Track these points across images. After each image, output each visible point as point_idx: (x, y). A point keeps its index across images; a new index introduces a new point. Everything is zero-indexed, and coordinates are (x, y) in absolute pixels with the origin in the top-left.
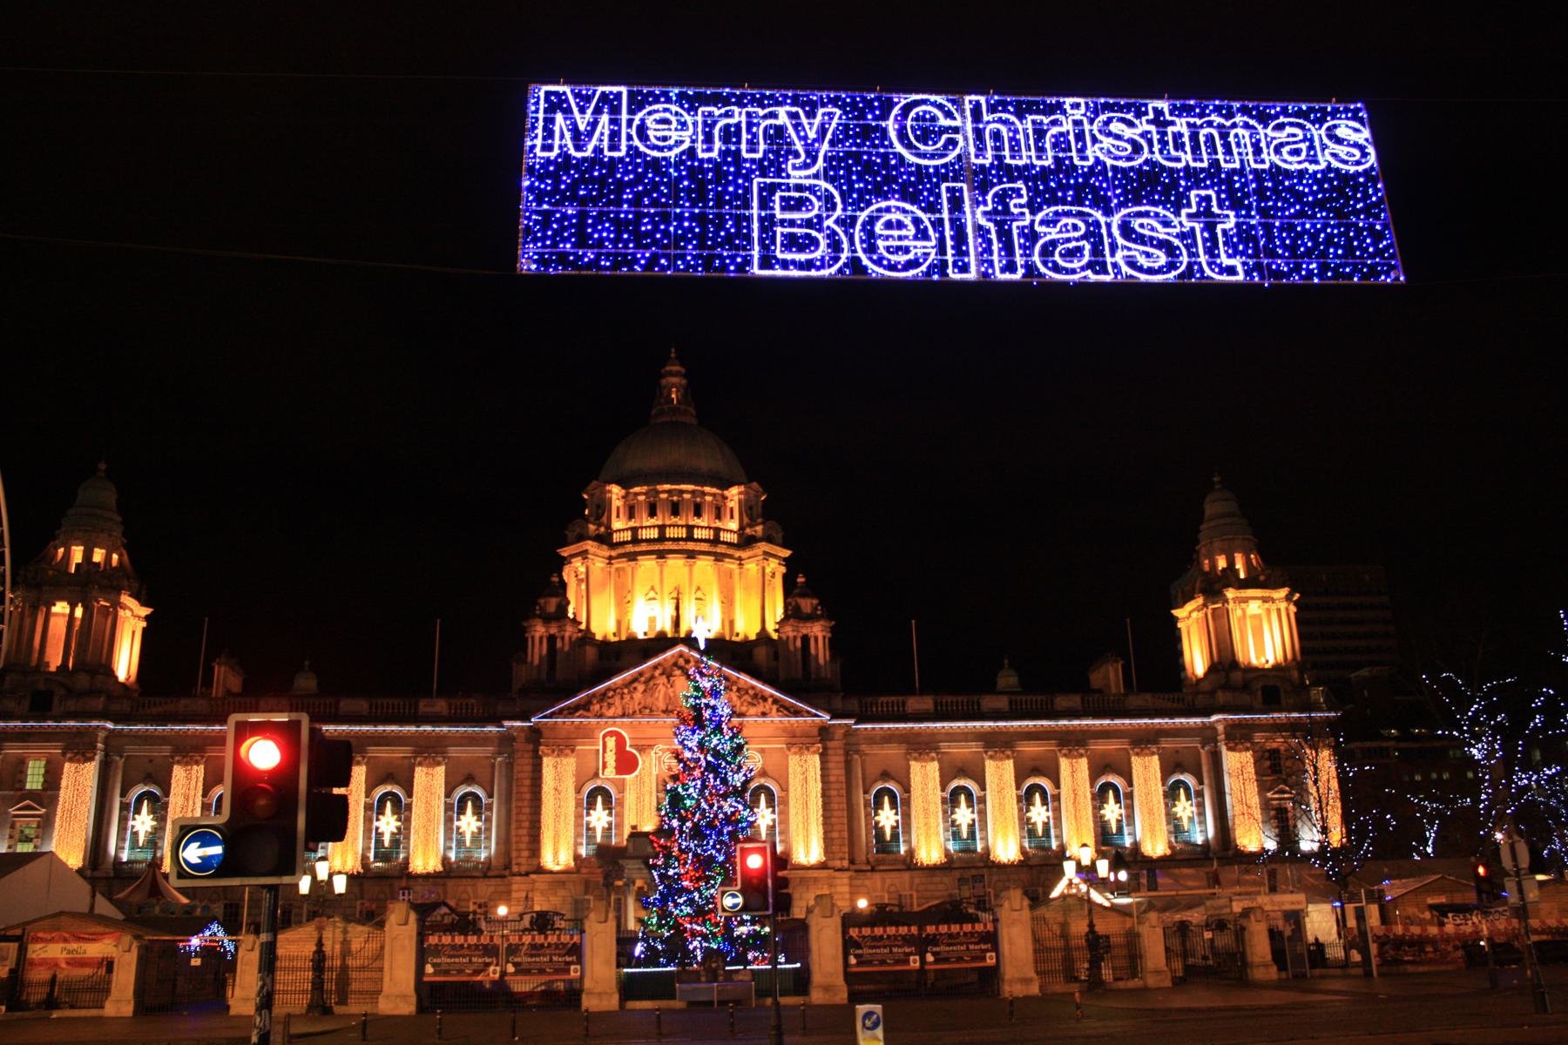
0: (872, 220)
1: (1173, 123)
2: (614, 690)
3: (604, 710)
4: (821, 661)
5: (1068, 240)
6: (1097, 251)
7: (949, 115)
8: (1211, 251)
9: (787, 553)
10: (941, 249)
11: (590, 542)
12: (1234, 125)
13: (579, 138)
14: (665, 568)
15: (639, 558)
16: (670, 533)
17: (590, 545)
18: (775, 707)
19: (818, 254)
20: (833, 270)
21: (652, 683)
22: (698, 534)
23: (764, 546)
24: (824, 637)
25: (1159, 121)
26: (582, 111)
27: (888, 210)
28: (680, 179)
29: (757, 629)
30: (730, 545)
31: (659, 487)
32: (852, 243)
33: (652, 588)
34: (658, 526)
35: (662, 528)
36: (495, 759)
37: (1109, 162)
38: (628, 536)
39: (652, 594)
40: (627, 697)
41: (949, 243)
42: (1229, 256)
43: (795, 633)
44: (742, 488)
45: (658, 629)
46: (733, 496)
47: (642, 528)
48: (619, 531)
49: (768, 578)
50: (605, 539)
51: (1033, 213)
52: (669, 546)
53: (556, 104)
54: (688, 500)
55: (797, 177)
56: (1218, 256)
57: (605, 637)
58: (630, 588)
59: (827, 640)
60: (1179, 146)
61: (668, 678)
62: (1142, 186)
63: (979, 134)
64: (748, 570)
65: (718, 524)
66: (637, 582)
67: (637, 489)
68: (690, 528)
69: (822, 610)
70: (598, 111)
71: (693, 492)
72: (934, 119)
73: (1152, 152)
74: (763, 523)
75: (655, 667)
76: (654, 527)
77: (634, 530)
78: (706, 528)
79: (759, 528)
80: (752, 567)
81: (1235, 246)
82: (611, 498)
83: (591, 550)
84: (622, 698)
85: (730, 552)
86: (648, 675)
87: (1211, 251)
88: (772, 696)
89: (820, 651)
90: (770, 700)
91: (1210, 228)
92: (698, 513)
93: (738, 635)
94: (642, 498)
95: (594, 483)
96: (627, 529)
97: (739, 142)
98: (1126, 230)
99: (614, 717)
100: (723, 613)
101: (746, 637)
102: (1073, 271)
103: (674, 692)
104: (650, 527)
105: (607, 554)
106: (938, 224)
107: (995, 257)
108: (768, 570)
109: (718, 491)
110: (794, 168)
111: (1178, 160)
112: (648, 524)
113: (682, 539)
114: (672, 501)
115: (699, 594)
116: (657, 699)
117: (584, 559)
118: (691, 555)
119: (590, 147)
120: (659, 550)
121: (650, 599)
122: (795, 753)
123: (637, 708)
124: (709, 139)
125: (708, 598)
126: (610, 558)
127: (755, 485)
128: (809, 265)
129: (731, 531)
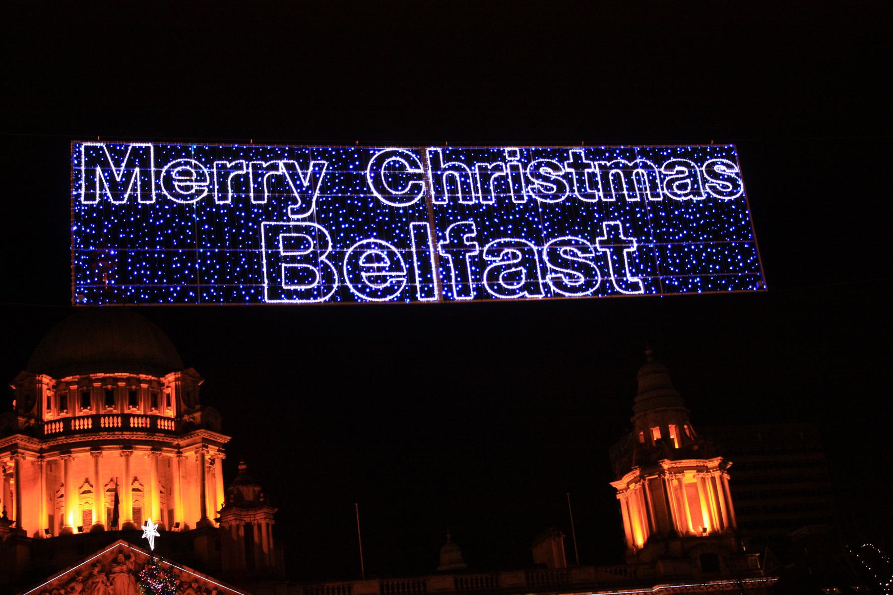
0: (356, 255)
1: (589, 166)
4: (265, 549)
5: (509, 267)
6: (531, 274)
7: (414, 164)
8: (619, 271)
10: (411, 277)
11: (20, 436)
12: (636, 166)
13: (117, 189)
14: (100, 459)
16: (105, 422)
17: (20, 439)
19: (315, 285)
20: (327, 298)
21: (90, 582)
22: (134, 423)
23: (202, 434)
24: (268, 525)
25: (578, 165)
26: (118, 164)
27: (368, 246)
28: (202, 223)
29: (198, 518)
30: (167, 432)
32: (341, 274)
33: (87, 481)
34: (92, 416)
35: (96, 418)
37: (539, 200)
38: (59, 427)
39: (86, 487)
41: (417, 272)
42: (633, 275)
43: (238, 522)
44: (179, 375)
45: (94, 522)
46: (169, 382)
47: (75, 418)
48: (51, 422)
49: (207, 465)
50: (36, 431)
51: (482, 245)
52: (105, 436)
53: (95, 158)
54: (122, 388)
55: (295, 219)
56: (625, 275)
57: (37, 533)
58: (63, 481)
59: (270, 528)
60: (593, 185)
61: (107, 575)
62: (565, 219)
63: (437, 179)
64: (187, 458)
65: (155, 412)
66: (71, 472)
67: (69, 379)
68: (126, 418)
69: (264, 497)
70: (130, 165)
71: (127, 380)
72: (403, 167)
73: (572, 191)
74: (201, 410)
75: (94, 565)
76: (88, 417)
77: (67, 421)
78: (142, 416)
79: (197, 415)
80: (190, 454)
81: (637, 266)
82: (41, 388)
83: (22, 443)
85: (168, 440)
86: (85, 574)
87: (619, 271)
88: (216, 588)
89: (264, 539)
91: (618, 252)
92: (134, 403)
93: (178, 525)
96: (59, 421)
97: (248, 191)
98: (554, 256)
100: (162, 503)
101: (186, 526)
102: (513, 292)
103: (114, 590)
104: (83, 417)
105: (37, 447)
106: (408, 257)
107: (453, 283)
108: (207, 457)
109: (153, 378)
110: (293, 212)
111: (592, 196)
112: (81, 414)
113: (117, 429)
114: (107, 389)
115: (137, 485)
117: (13, 453)
118: (127, 446)
119: (126, 196)
120: (93, 441)
121: (84, 492)
124: (223, 189)
125: (146, 488)
126: (41, 451)
127: (192, 370)
128: (307, 294)
129: (168, 419)
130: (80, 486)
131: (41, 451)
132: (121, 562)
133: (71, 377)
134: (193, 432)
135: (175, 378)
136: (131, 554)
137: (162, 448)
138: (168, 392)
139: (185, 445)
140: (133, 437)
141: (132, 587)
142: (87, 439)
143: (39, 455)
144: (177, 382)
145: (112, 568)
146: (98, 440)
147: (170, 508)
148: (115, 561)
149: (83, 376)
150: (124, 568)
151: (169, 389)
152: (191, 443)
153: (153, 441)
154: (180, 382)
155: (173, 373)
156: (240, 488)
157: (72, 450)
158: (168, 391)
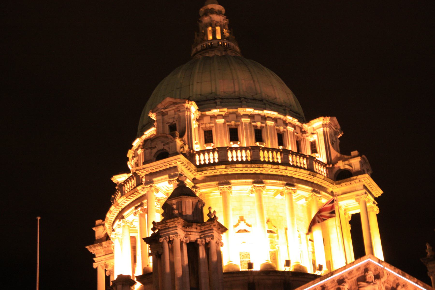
15: (232, 181)
31: (241, 111)
44: (327, 120)
67: (215, 112)
71: (275, 120)
82: (190, 116)
95: (168, 100)
109: (298, 123)
114: (255, 127)
120: (255, 174)
121: (239, 231)
130: (235, 224)
132: (371, 281)
133: (218, 110)
134: (355, 177)
135: (323, 125)
136: (385, 272)
137: (321, 192)
139: (340, 193)
140: (295, 175)
142: (249, 172)
144: (325, 128)
145: (361, 287)
146: (261, 174)
147: (330, 259)
149: (231, 110)
152: (348, 191)
153: (312, 183)
154: (328, 129)
155: (322, 118)
158: (311, 139)
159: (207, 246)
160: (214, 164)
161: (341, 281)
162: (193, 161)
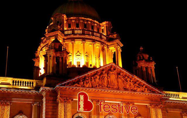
2: (88, 77)
3: (85, 84)
9: (122, 45)
18: (146, 89)
36: (33, 104)
40: (93, 81)
44: (107, 22)
61: (107, 75)
67: (72, 18)
71: (91, 21)
79: (115, 36)
84: (91, 81)
88: (144, 85)
90: (144, 86)
94: (73, 21)
99: (89, 88)
109: (98, 23)
114: (85, 23)
116: (104, 82)
121: (77, 55)
122: (153, 108)
123: (97, 85)
127: (110, 22)
131: (64, 39)
133: (73, 18)
138: (102, 28)
141: (116, 80)
143: (63, 40)
148: (110, 70)
150: (114, 73)
151: (103, 27)
153: (101, 41)
156: (143, 55)
157: (76, 40)
158: (102, 28)
159: (62, 58)
160: (70, 34)
161: (103, 70)
162: (64, 33)
